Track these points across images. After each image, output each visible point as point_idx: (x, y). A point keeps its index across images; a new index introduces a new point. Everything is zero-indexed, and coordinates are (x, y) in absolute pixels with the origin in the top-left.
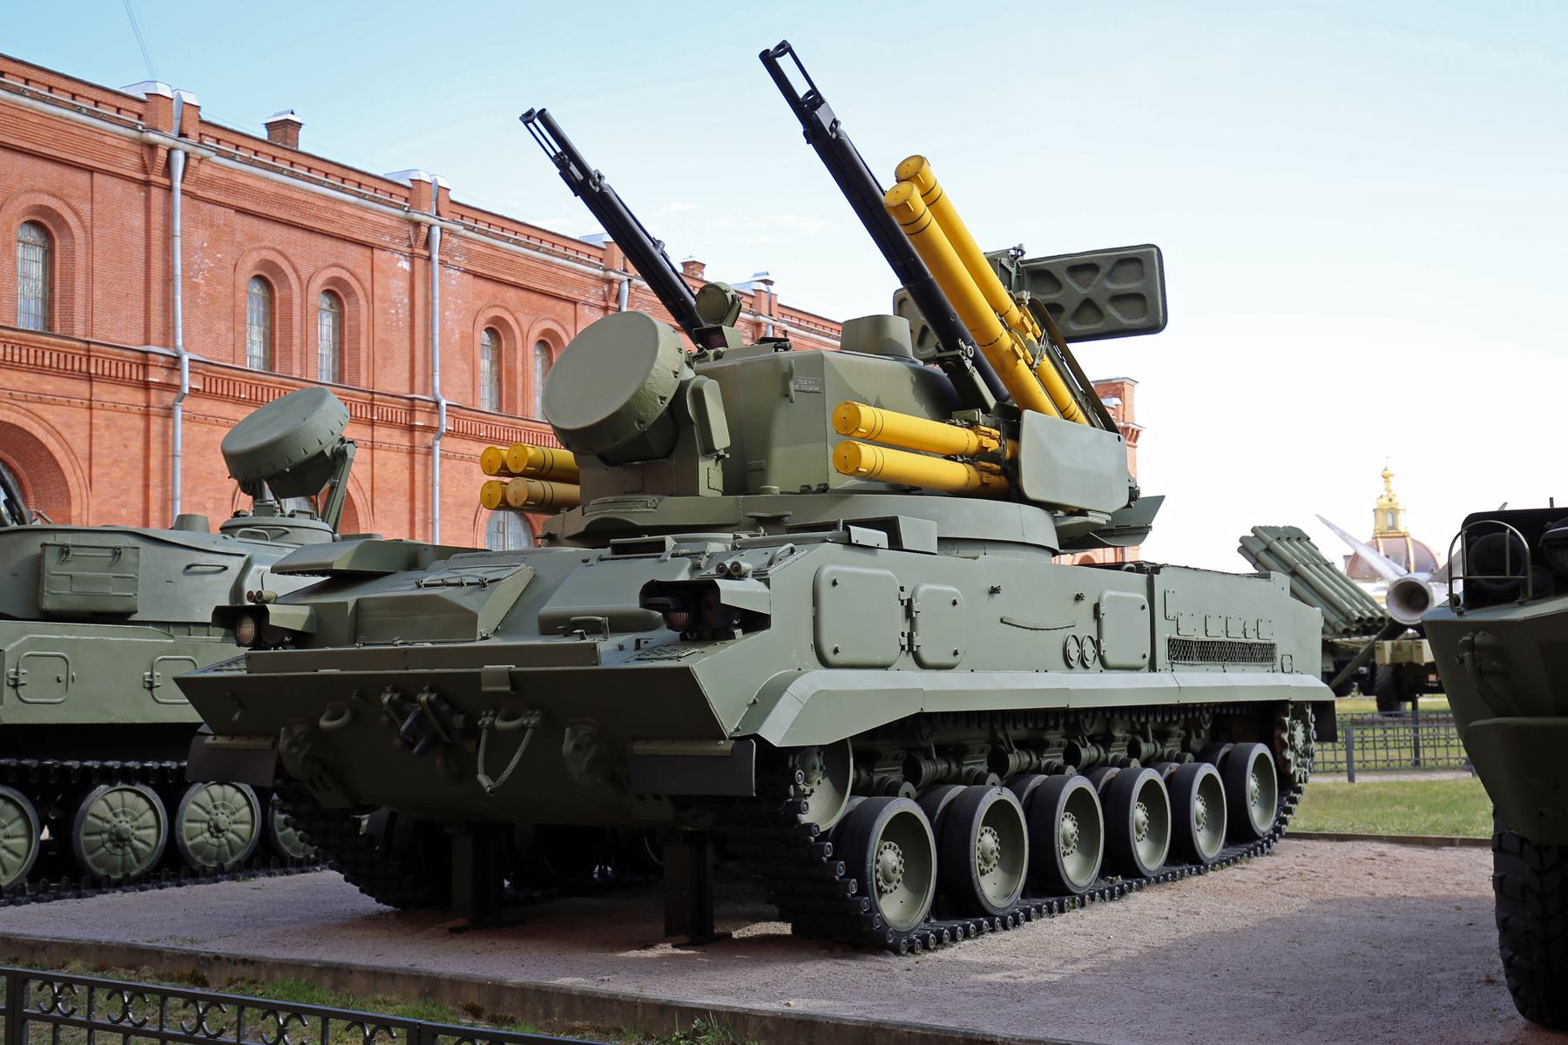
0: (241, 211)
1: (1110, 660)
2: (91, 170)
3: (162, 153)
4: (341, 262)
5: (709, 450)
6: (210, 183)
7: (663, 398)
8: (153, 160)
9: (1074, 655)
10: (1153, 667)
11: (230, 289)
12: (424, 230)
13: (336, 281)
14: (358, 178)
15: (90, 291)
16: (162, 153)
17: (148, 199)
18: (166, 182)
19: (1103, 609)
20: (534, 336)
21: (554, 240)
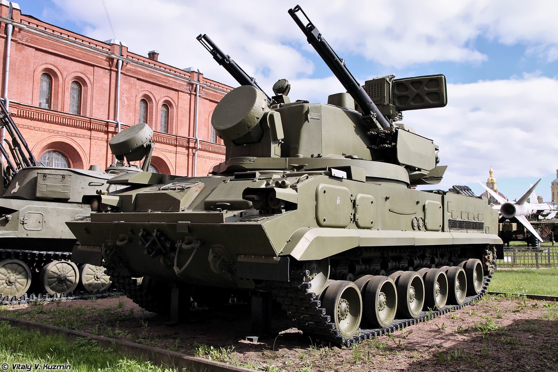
0: (138, 79)
1: (429, 227)
2: (93, 66)
3: (115, 61)
5: (275, 140)
6: (129, 70)
7: (258, 118)
8: (112, 63)
9: (415, 225)
10: (443, 230)
12: (195, 86)
13: (166, 101)
15: (92, 102)
16: (115, 61)
17: (110, 75)
18: (116, 70)
19: (426, 207)
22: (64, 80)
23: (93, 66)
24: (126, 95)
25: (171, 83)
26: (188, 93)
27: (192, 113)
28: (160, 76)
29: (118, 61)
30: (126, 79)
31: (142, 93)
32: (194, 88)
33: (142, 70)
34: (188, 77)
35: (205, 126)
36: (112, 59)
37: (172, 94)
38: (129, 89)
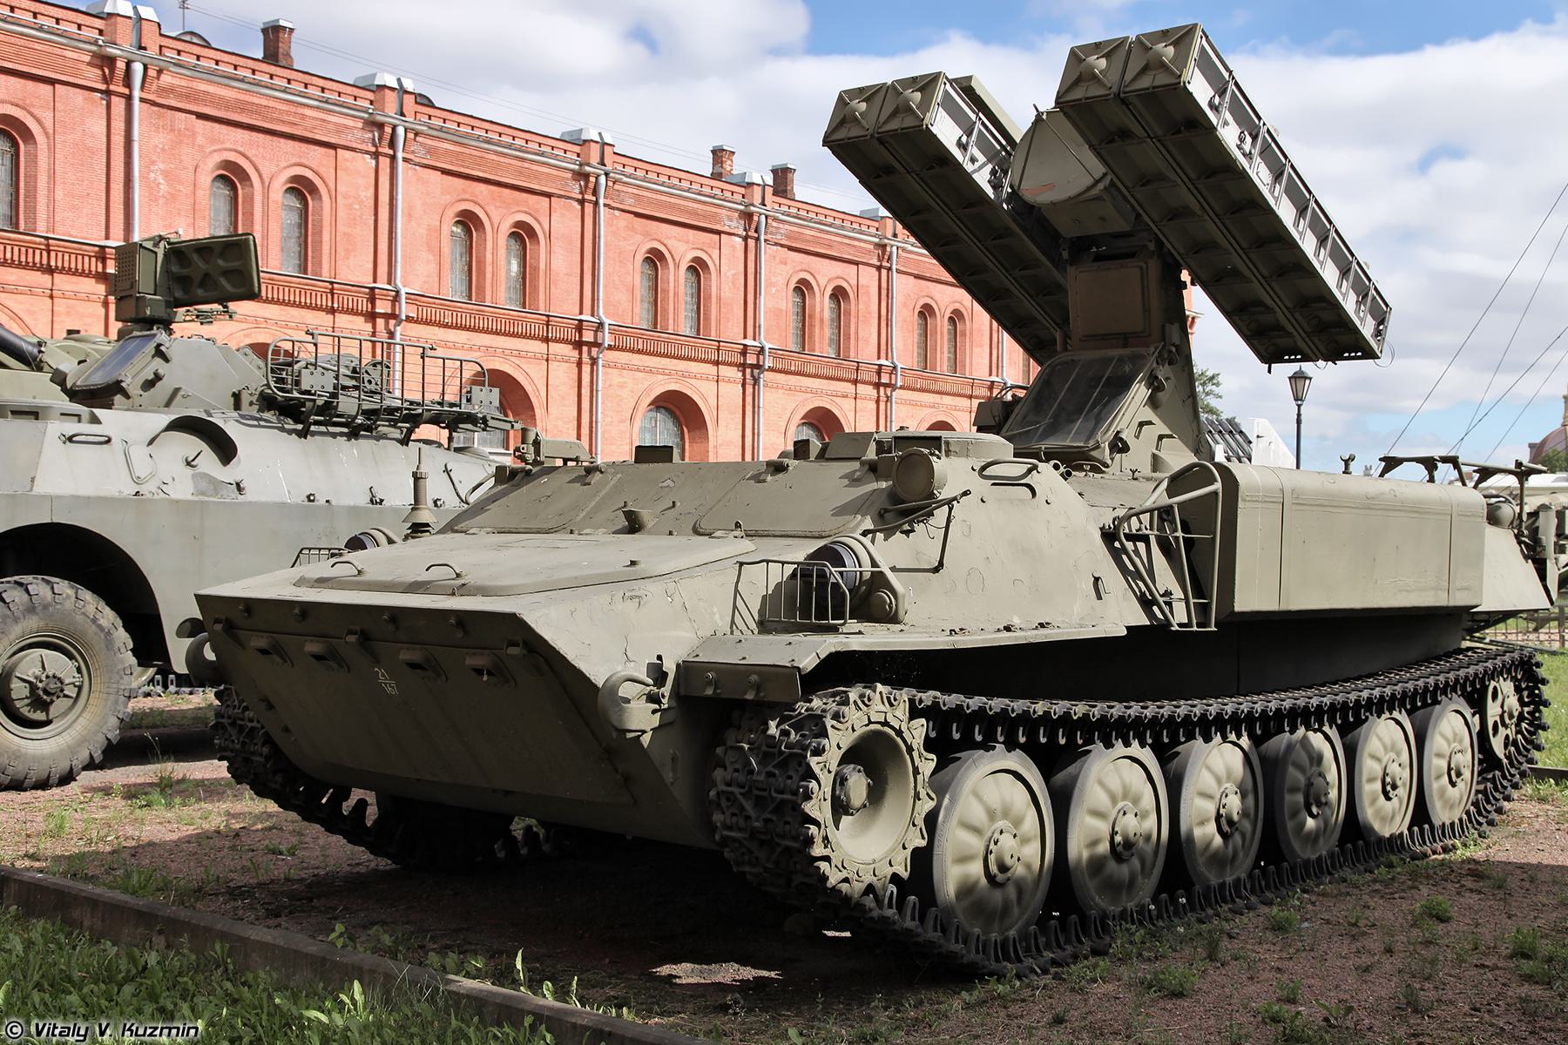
0: (201, 116)
2: (52, 82)
3: (121, 65)
8: (112, 71)
12: (388, 130)
13: (297, 179)
14: (321, 83)
15: (51, 190)
16: (121, 65)
18: (126, 91)
20: (506, 228)
21: (528, 136)
23: (52, 82)
24: (162, 166)
25: (309, 123)
26: (367, 152)
27: (384, 211)
28: (272, 104)
29: (129, 64)
30: (160, 116)
31: (218, 158)
32: (387, 137)
33: (211, 89)
34: (367, 104)
35: (430, 249)
36: (110, 61)
37: (316, 155)
38: (172, 148)
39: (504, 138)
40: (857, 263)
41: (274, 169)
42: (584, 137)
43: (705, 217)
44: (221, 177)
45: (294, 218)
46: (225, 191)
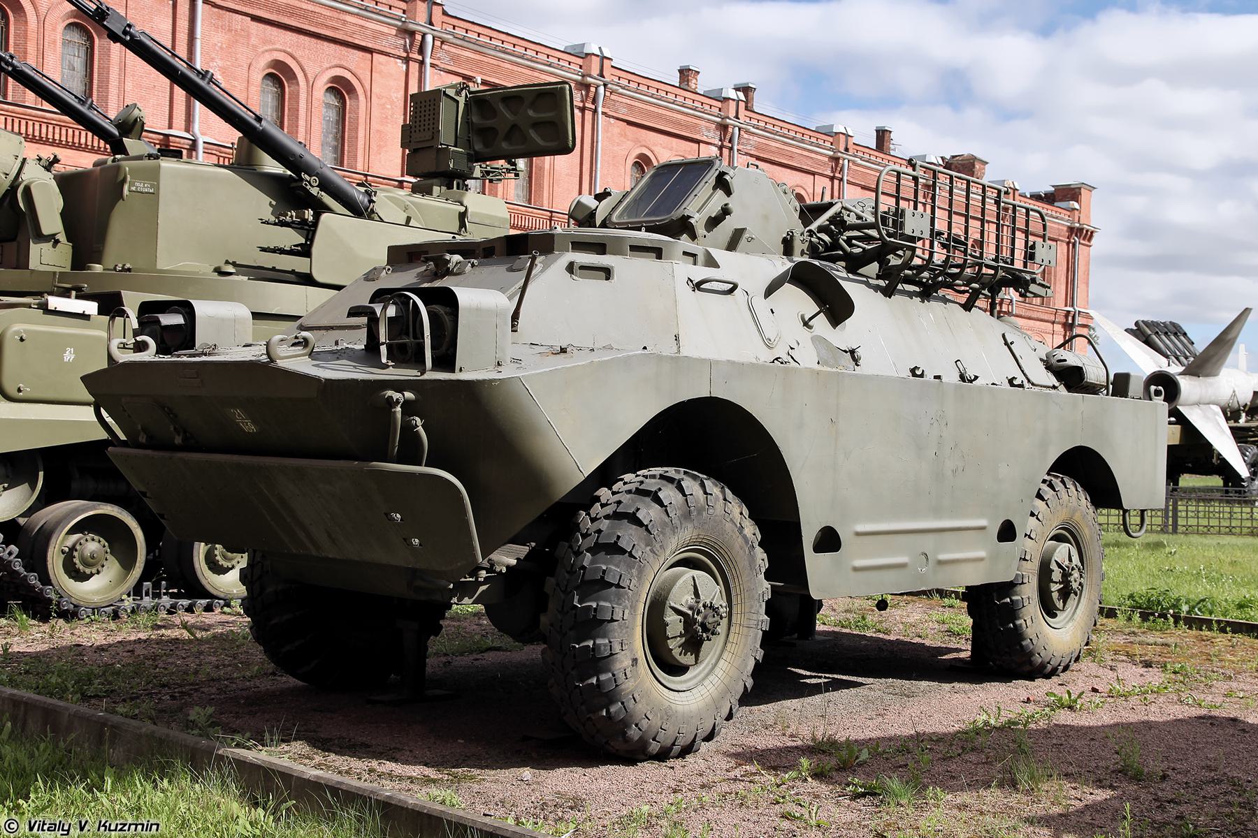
0: (255, 19)
4: (345, 64)
11: (245, 85)
12: (419, 37)
13: (336, 79)
15: (122, 82)
21: (538, 48)
22: (42, 22)
24: (220, 63)
25: (349, 28)
26: (399, 57)
30: (219, 17)
31: (269, 58)
32: (417, 43)
34: (400, 13)
38: (229, 47)
39: (517, 49)
40: (813, 174)
41: (318, 70)
42: (586, 51)
43: (687, 127)
44: (270, 75)
45: (332, 115)
46: (272, 89)
